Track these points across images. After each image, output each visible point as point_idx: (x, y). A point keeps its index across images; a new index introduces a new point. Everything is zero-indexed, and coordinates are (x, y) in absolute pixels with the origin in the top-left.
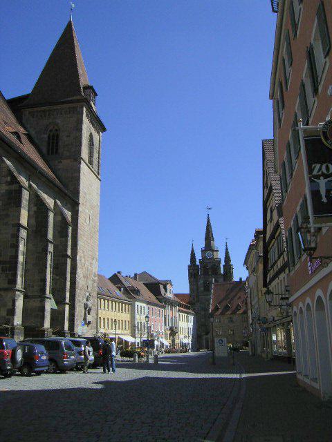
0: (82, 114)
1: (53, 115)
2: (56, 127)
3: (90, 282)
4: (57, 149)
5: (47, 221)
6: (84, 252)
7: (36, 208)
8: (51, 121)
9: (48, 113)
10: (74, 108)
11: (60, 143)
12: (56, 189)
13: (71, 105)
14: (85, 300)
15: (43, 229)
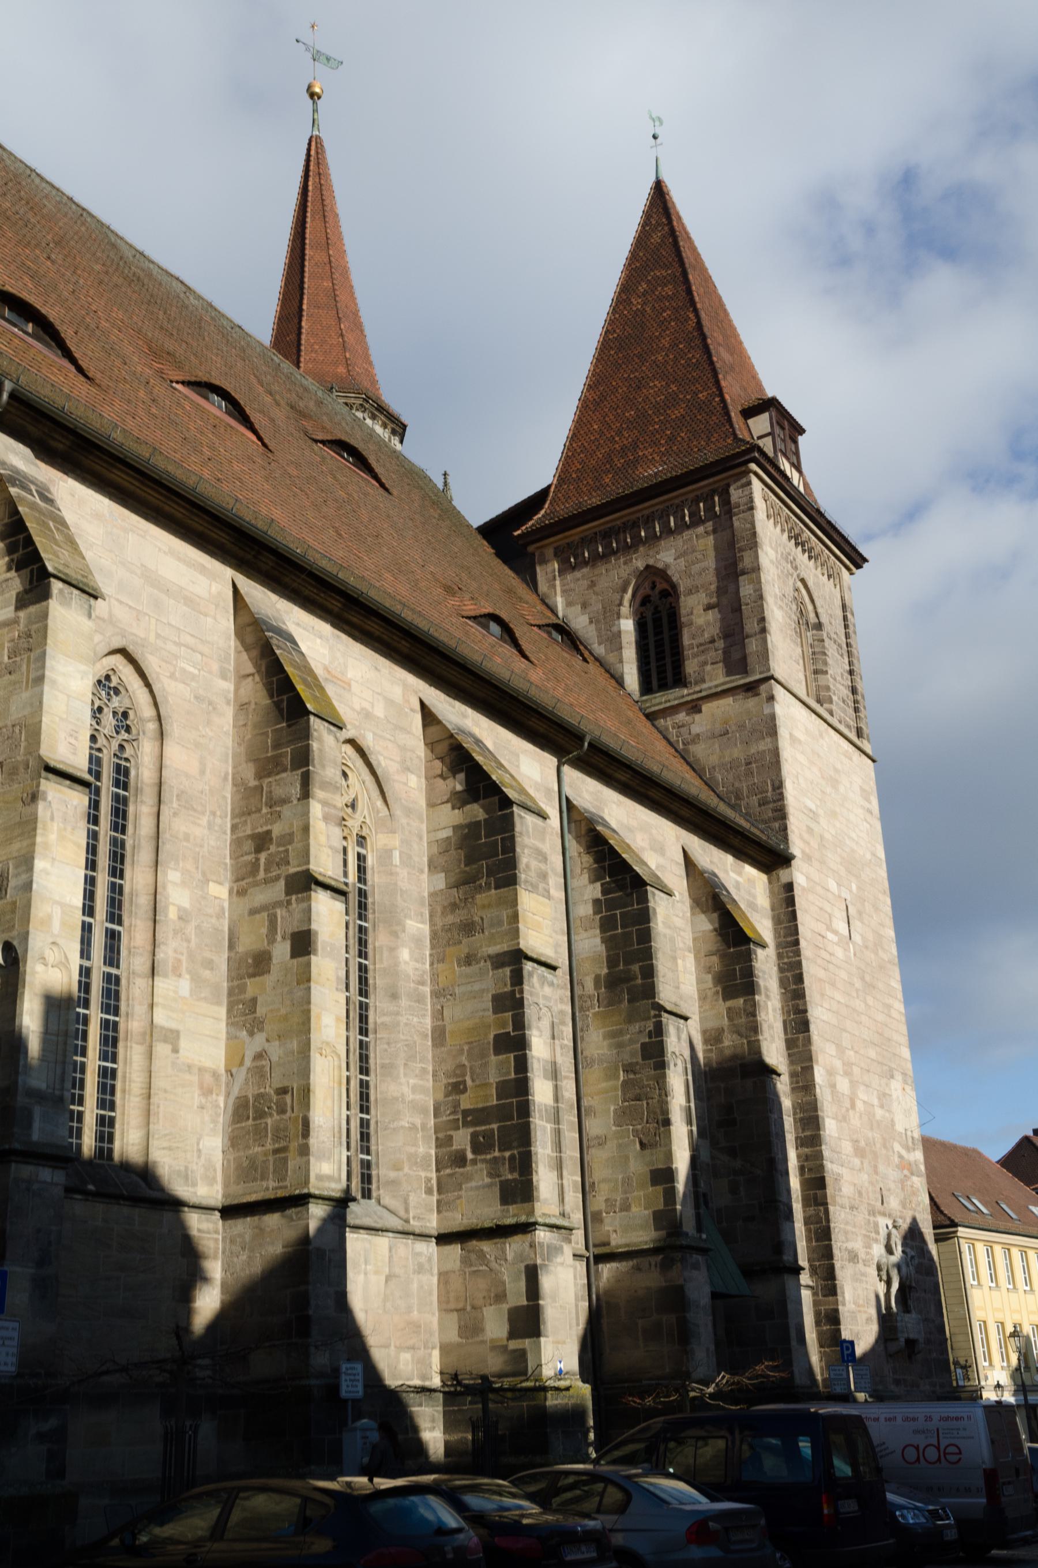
3: (893, 1175)
6: (841, 1050)
15: (636, 968)
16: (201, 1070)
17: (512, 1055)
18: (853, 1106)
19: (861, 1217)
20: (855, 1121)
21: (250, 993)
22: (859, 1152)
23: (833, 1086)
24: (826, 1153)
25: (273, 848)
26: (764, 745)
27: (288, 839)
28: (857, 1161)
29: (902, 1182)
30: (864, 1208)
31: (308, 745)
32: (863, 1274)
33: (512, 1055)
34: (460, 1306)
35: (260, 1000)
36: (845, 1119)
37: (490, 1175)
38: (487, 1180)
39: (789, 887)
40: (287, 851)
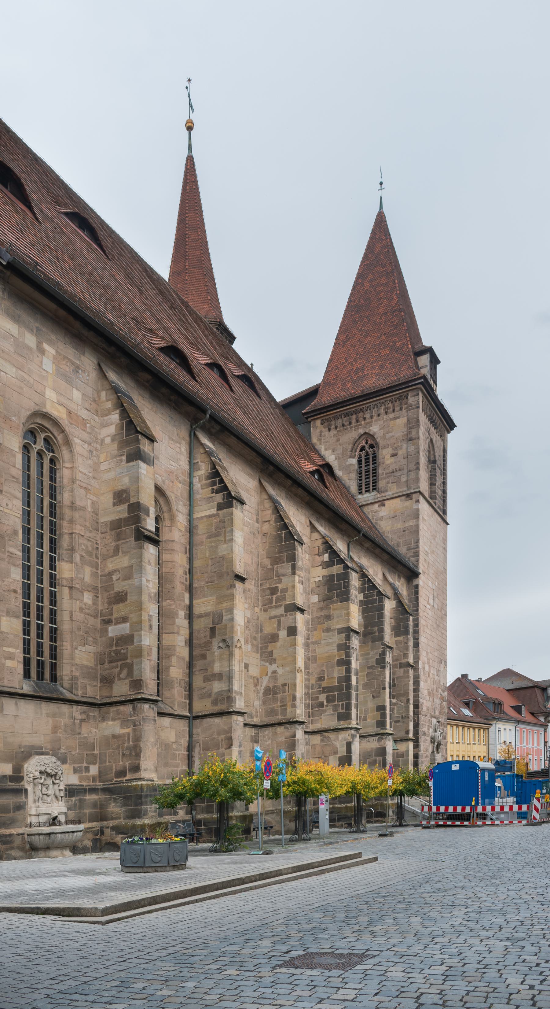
3: (437, 701)
4: (375, 482)
5: (381, 616)
6: (427, 653)
7: (362, 595)
11: (380, 471)
12: (386, 557)
14: (431, 730)
15: (376, 629)
16: (254, 677)
17: (344, 668)
18: (429, 676)
19: (428, 718)
20: (429, 682)
21: (269, 649)
22: (429, 694)
23: (424, 668)
24: (420, 695)
25: (279, 594)
26: (412, 523)
27: (286, 590)
28: (428, 697)
29: (441, 704)
30: (428, 716)
31: (295, 553)
32: (426, 740)
33: (344, 668)
34: (320, 756)
35: (274, 652)
36: (426, 681)
37: (334, 710)
38: (332, 712)
39: (417, 586)
40: (285, 595)
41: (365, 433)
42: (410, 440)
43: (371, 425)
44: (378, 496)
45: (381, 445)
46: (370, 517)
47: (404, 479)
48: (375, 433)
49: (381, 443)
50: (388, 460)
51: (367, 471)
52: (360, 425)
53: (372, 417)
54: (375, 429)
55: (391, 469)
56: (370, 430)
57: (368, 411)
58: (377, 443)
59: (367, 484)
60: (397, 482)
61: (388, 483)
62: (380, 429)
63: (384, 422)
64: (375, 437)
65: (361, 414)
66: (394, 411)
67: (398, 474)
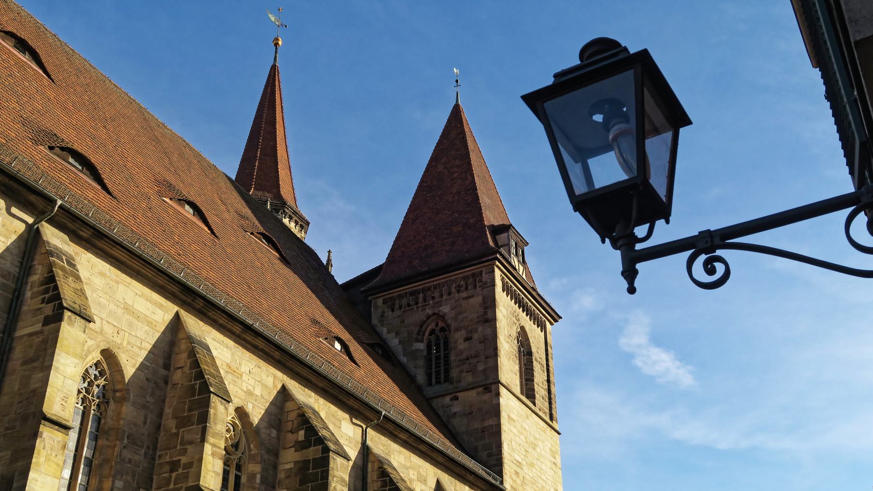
0: (493, 285)
1: (433, 298)
2: (441, 324)
4: (447, 371)
8: (429, 311)
9: (421, 296)
10: (474, 275)
11: (453, 357)
13: (468, 271)
41: (434, 314)
42: (487, 321)
43: (440, 304)
44: (450, 386)
45: (452, 328)
46: (440, 413)
47: (481, 367)
48: (445, 314)
49: (453, 325)
50: (462, 346)
51: (438, 358)
52: (429, 304)
53: (441, 296)
54: (445, 309)
55: (464, 356)
56: (439, 311)
57: (437, 290)
58: (448, 326)
59: (438, 373)
60: (473, 370)
61: (462, 372)
62: (452, 309)
63: (456, 301)
64: (446, 318)
65: (429, 293)
66: (466, 289)
67: (475, 360)
